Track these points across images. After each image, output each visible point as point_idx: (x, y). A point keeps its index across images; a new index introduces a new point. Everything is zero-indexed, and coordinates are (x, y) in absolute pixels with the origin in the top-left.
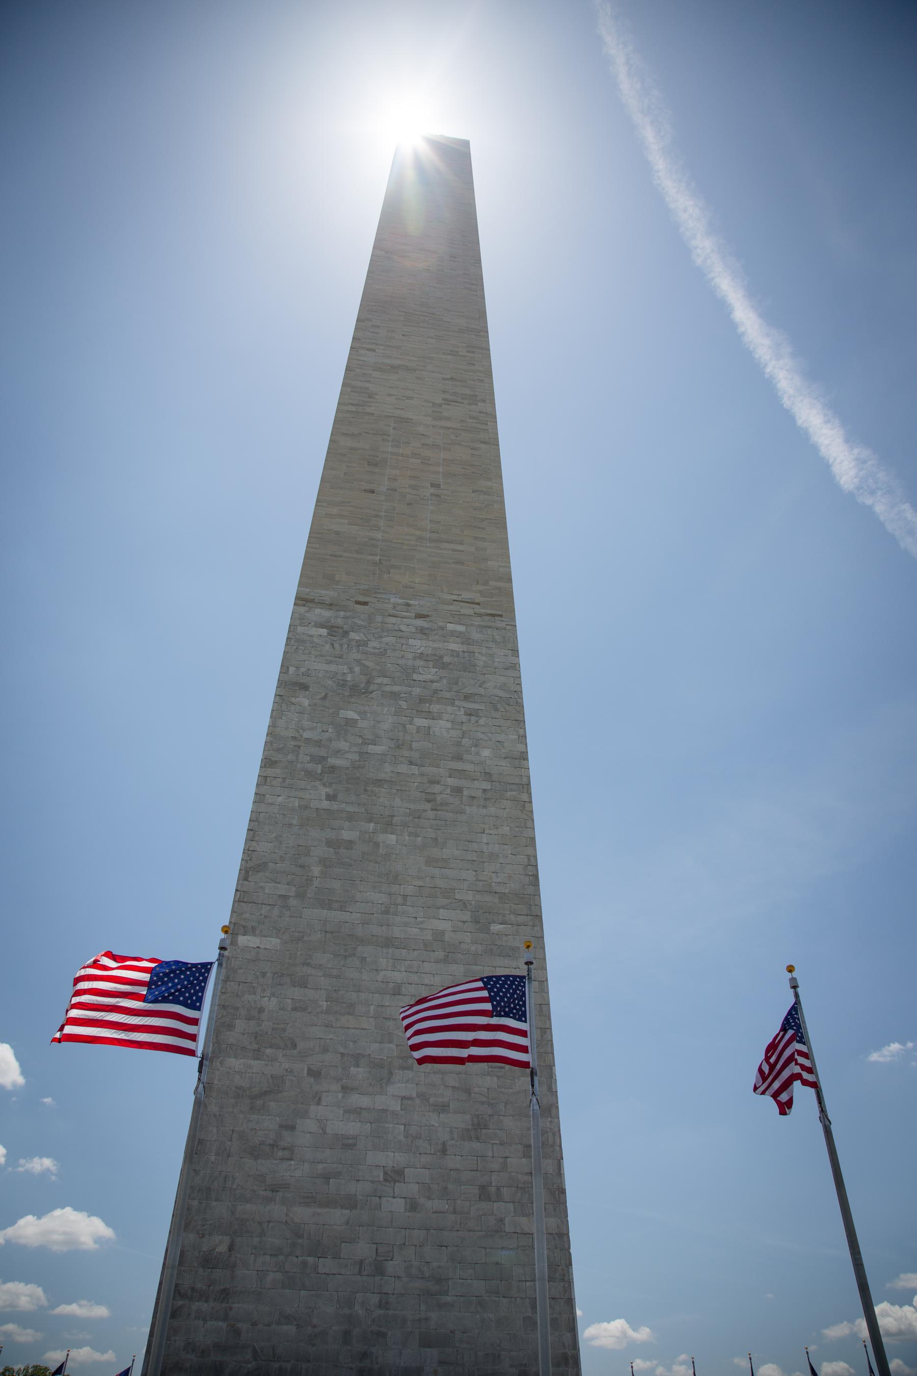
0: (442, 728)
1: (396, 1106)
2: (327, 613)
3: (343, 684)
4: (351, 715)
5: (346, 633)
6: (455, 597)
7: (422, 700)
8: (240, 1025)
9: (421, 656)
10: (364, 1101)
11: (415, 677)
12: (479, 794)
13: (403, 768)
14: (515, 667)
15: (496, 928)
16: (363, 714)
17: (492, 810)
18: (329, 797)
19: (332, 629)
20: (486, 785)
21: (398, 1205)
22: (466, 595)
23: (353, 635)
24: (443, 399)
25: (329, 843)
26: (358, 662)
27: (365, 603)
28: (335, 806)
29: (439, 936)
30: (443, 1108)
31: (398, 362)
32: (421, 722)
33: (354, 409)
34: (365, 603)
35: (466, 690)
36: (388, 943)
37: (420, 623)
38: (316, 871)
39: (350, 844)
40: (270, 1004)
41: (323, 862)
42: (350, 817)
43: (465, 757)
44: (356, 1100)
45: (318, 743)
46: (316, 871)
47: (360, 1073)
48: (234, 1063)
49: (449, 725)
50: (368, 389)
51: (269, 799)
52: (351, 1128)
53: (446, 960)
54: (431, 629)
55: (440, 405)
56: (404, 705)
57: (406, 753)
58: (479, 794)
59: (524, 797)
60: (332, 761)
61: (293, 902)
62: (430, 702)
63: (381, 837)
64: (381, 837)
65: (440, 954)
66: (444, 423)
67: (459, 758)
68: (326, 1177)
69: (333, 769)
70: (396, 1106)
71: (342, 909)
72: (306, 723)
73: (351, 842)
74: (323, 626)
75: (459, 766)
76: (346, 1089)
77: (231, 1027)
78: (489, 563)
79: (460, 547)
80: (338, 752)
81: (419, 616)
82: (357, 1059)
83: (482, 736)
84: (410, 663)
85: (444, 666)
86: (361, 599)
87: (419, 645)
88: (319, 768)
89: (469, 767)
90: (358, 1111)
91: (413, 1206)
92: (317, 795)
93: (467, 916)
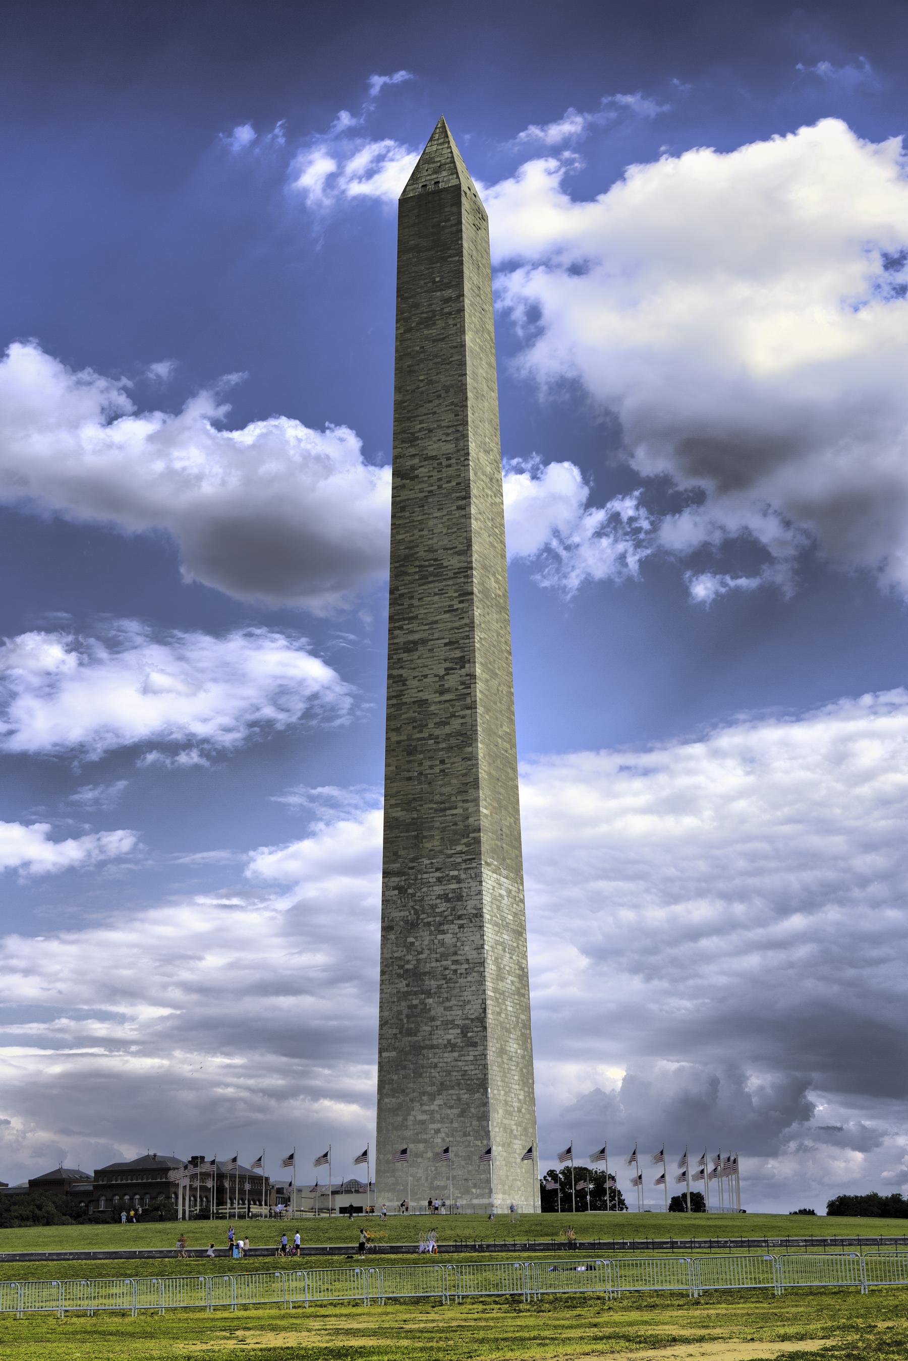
0: (448, 938)
1: (437, 1108)
2: (397, 879)
3: (407, 922)
5: (406, 890)
6: (453, 852)
7: (441, 924)
8: (387, 1086)
9: (439, 897)
10: (427, 1108)
11: (437, 910)
12: (464, 971)
14: (480, 893)
15: (469, 1035)
16: (416, 938)
17: (469, 979)
18: (407, 985)
20: (467, 966)
21: (439, 1140)
23: (410, 891)
24: (446, 669)
25: (409, 1007)
26: (412, 907)
27: (412, 868)
29: (449, 1041)
30: (451, 1107)
31: (416, 637)
32: (440, 937)
33: (394, 701)
34: (412, 868)
35: (460, 913)
36: (432, 1047)
37: (438, 874)
38: (405, 1021)
39: (416, 1006)
40: (395, 1077)
41: (408, 1016)
42: (416, 993)
43: (459, 952)
44: (426, 1108)
45: (399, 958)
46: (405, 1021)
47: (425, 1098)
48: (387, 1100)
49: (451, 936)
50: (401, 675)
51: (385, 991)
52: (424, 1117)
53: (452, 1051)
54: (443, 877)
55: (443, 677)
56: (432, 928)
57: (435, 956)
58: (464, 971)
59: (482, 969)
60: (407, 967)
61: (399, 1036)
62: (443, 924)
63: (427, 1001)
64: (427, 1001)
65: (450, 1049)
66: (447, 697)
67: (455, 953)
68: (417, 1134)
69: (407, 971)
70: (437, 1108)
71: (415, 1036)
72: (395, 949)
73: (416, 1005)
74: (394, 888)
75: (455, 958)
76: (421, 1105)
77: (384, 1088)
78: (470, 819)
79: (455, 812)
80: (408, 962)
81: (437, 870)
82: (424, 1093)
83: (464, 939)
84: (434, 902)
85: (448, 900)
86: (411, 865)
87: (438, 890)
88: (402, 972)
89: (459, 958)
90: (425, 1112)
91: (443, 1140)
92: (402, 985)
93: (459, 1031)
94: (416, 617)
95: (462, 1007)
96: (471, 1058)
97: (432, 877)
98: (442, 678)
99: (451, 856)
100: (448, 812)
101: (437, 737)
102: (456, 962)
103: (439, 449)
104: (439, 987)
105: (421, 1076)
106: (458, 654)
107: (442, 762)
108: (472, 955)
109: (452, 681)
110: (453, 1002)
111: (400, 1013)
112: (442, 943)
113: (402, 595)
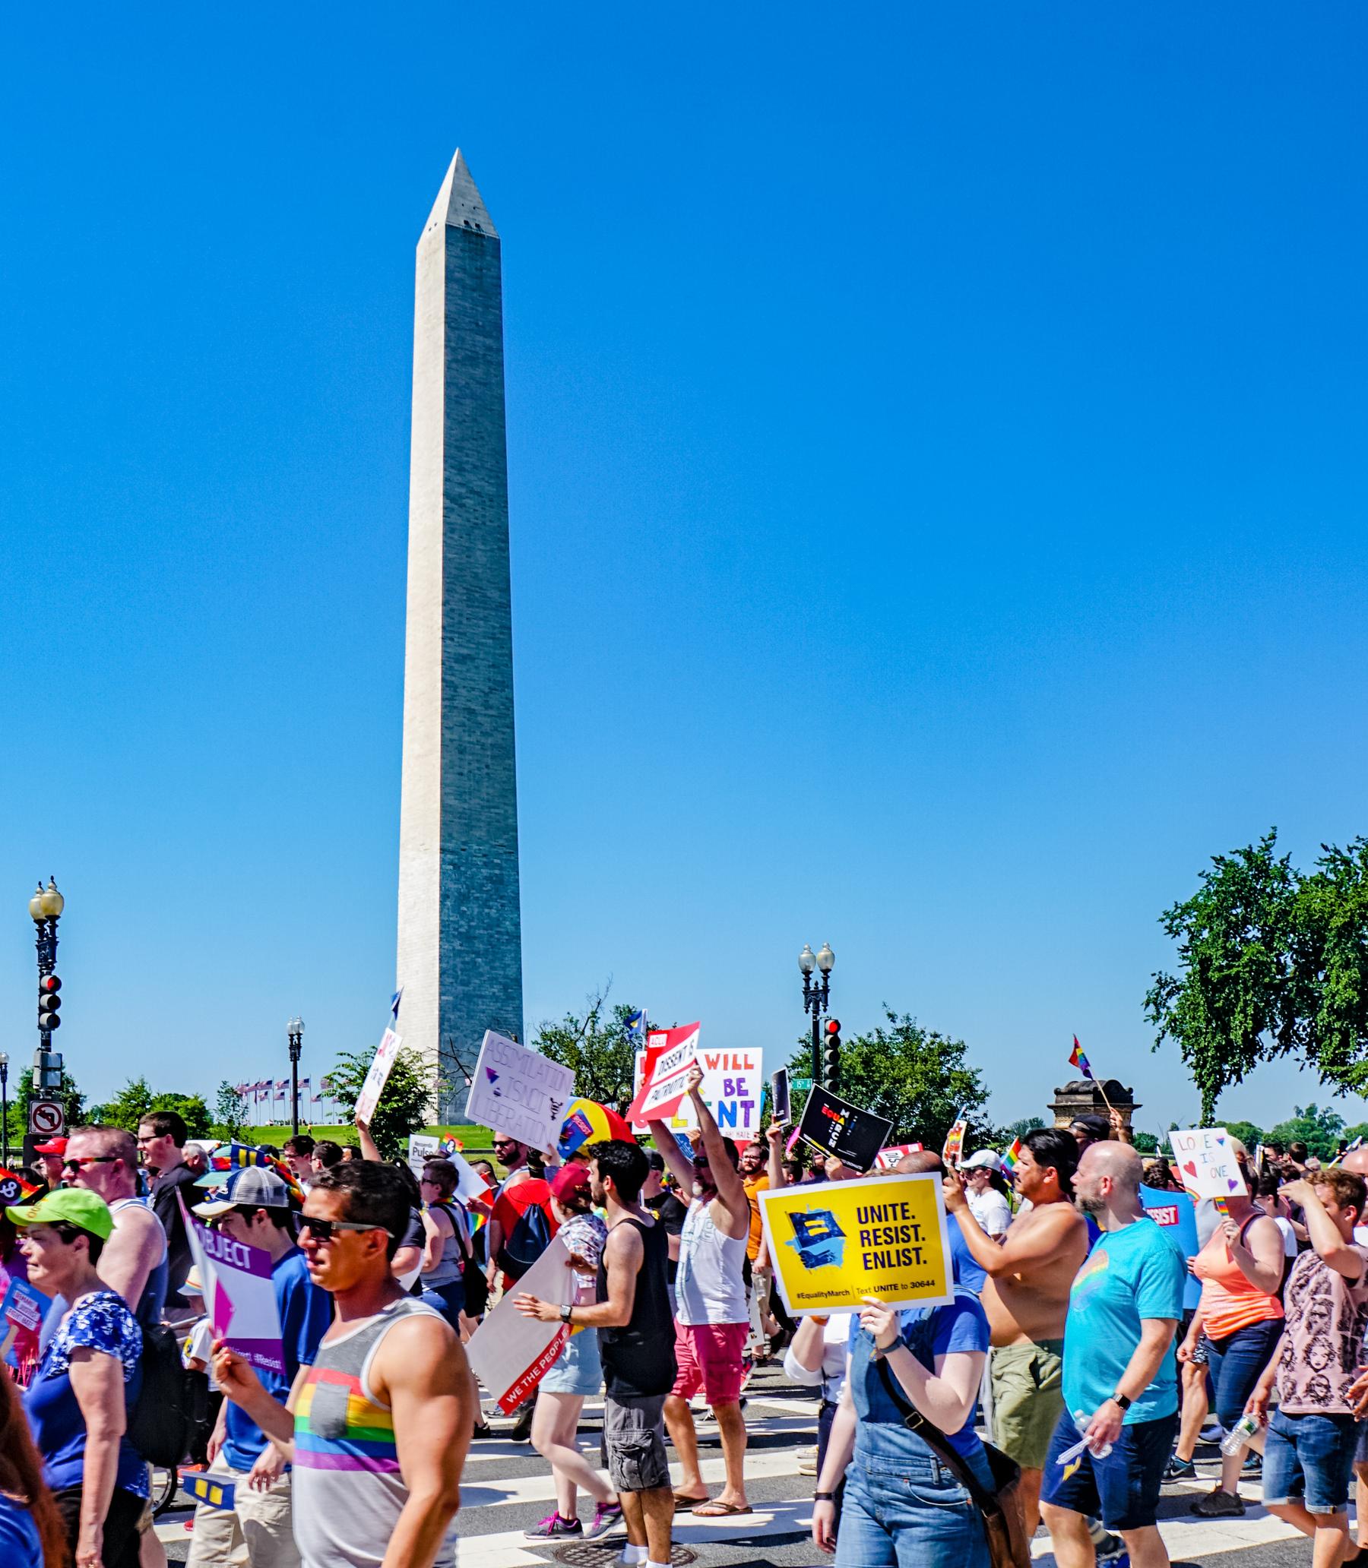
3: (460, 893)
9: (485, 878)
19: (454, 865)
22: (501, 842)
36: (481, 997)
69: (460, 933)
85: (493, 882)
87: (485, 872)
94: (465, 634)
95: (504, 969)
97: (479, 861)
98: (486, 694)
99: (494, 846)
102: (498, 933)
103: (482, 487)
104: (487, 950)
105: (472, 1018)
106: (499, 678)
107: (487, 767)
108: (511, 928)
109: (493, 700)
110: (497, 964)
111: (455, 966)
113: (452, 610)
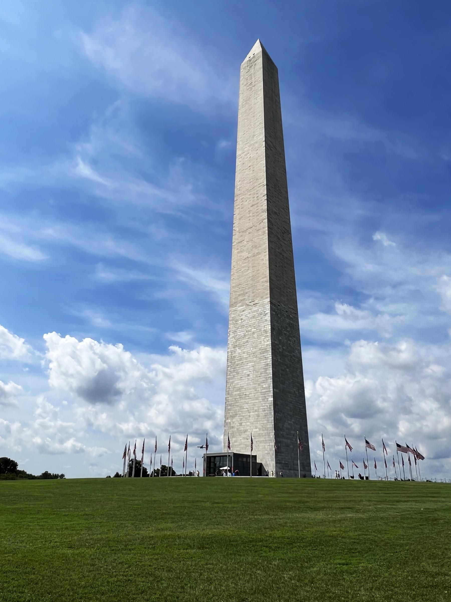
4: (280, 338)
13: (288, 353)
19: (276, 312)
27: (279, 306)
28: (281, 361)
30: (297, 424)
32: (289, 342)
37: (287, 313)
41: (281, 374)
52: (289, 427)
53: (295, 397)
60: (280, 350)
67: (294, 352)
76: (288, 420)
81: (287, 312)
90: (289, 424)
96: (301, 402)
100: (288, 289)
101: (283, 256)
112: (290, 344)
